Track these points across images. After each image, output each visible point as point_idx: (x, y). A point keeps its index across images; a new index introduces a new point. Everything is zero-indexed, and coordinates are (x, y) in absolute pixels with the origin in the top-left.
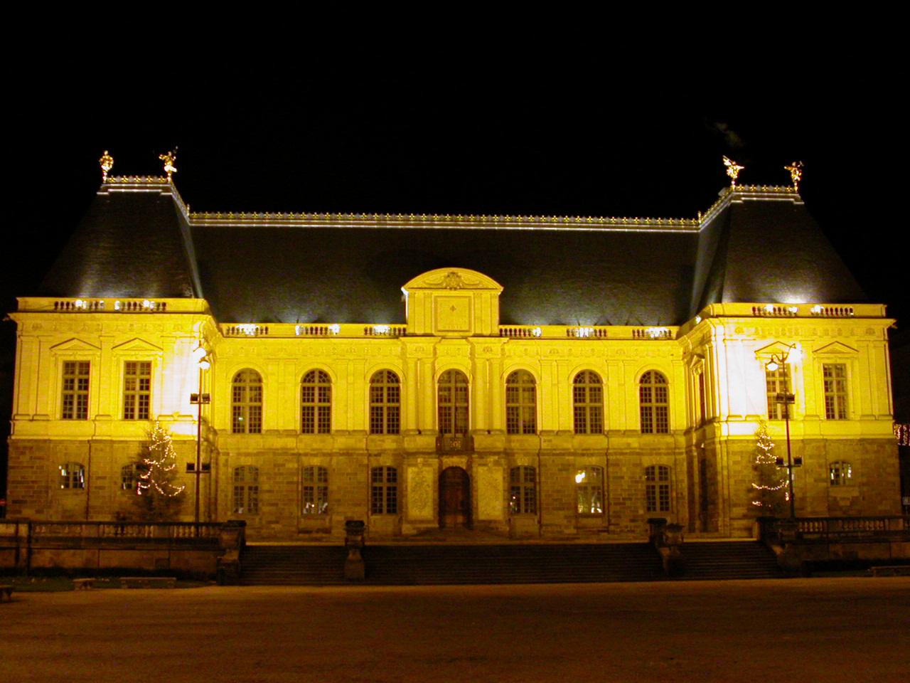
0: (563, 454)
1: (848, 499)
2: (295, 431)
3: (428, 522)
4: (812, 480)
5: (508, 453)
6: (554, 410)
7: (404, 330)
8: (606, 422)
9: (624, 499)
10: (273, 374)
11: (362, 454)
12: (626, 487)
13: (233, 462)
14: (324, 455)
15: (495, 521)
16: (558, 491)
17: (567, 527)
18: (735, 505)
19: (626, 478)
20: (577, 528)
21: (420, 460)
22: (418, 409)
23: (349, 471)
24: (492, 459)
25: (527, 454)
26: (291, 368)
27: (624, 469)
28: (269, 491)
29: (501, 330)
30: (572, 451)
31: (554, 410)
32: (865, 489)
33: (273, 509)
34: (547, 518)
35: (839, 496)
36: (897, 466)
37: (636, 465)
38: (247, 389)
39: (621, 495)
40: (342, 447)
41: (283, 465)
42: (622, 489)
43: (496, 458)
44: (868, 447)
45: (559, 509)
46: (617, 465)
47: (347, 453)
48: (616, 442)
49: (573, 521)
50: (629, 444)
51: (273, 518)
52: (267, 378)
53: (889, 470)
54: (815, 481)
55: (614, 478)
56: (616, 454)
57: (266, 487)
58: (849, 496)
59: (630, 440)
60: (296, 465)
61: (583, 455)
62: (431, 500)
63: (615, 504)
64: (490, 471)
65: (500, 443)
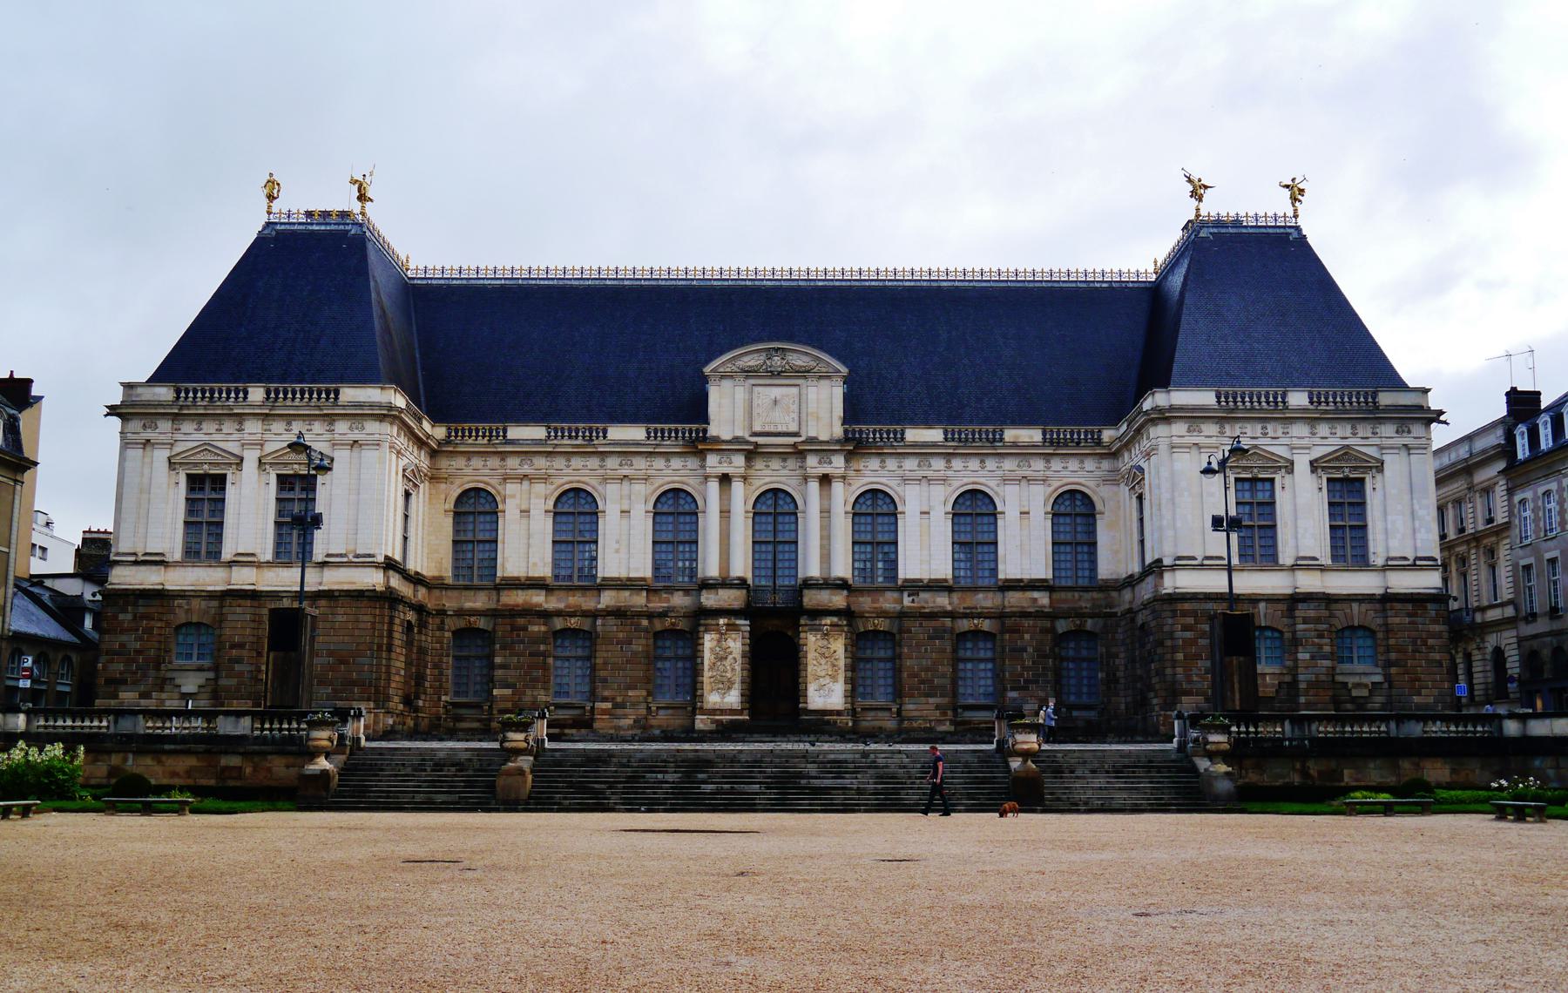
0: (933, 616)
1: (1366, 686)
2: (543, 579)
3: (732, 712)
4: (1307, 656)
5: (848, 614)
6: (925, 550)
7: (705, 431)
8: (1001, 567)
9: (1027, 681)
10: (513, 496)
11: (640, 615)
12: (1028, 663)
13: (452, 623)
14: (585, 614)
15: (831, 712)
16: (927, 669)
17: (939, 722)
18: (1188, 693)
19: (1030, 650)
20: (953, 722)
21: (722, 621)
22: (727, 547)
23: (621, 635)
24: (828, 621)
25: (883, 614)
26: (540, 488)
27: (1027, 636)
28: (503, 666)
29: (846, 431)
30: (949, 608)
31: (925, 550)
32: (1393, 670)
33: (508, 692)
34: (910, 707)
35: (1351, 680)
36: (1446, 635)
37: (1044, 631)
38: (475, 514)
39: (1021, 675)
40: (612, 603)
41: (525, 629)
42: (1023, 668)
43: (835, 619)
44: (1398, 606)
45: (928, 695)
46: (1015, 630)
47: (618, 613)
48: (1015, 599)
49: (950, 713)
50: (1035, 600)
51: (509, 705)
52: (504, 501)
53: (1430, 642)
54: (1313, 658)
55: (1013, 650)
56: (1013, 615)
57: (498, 660)
58: (1365, 680)
59: (1036, 595)
60: (543, 628)
61: (965, 616)
62: (738, 679)
63: (1013, 689)
64: (826, 635)
65: (838, 600)
